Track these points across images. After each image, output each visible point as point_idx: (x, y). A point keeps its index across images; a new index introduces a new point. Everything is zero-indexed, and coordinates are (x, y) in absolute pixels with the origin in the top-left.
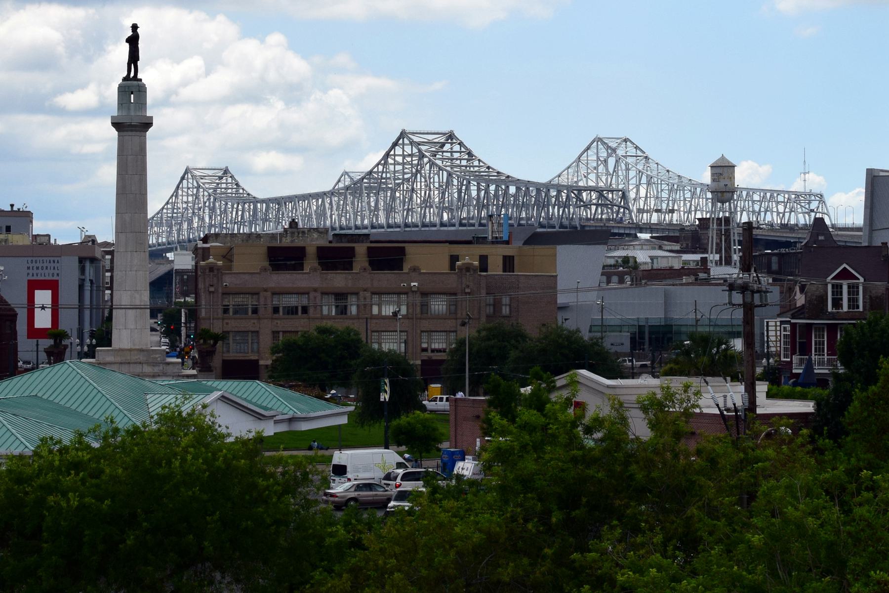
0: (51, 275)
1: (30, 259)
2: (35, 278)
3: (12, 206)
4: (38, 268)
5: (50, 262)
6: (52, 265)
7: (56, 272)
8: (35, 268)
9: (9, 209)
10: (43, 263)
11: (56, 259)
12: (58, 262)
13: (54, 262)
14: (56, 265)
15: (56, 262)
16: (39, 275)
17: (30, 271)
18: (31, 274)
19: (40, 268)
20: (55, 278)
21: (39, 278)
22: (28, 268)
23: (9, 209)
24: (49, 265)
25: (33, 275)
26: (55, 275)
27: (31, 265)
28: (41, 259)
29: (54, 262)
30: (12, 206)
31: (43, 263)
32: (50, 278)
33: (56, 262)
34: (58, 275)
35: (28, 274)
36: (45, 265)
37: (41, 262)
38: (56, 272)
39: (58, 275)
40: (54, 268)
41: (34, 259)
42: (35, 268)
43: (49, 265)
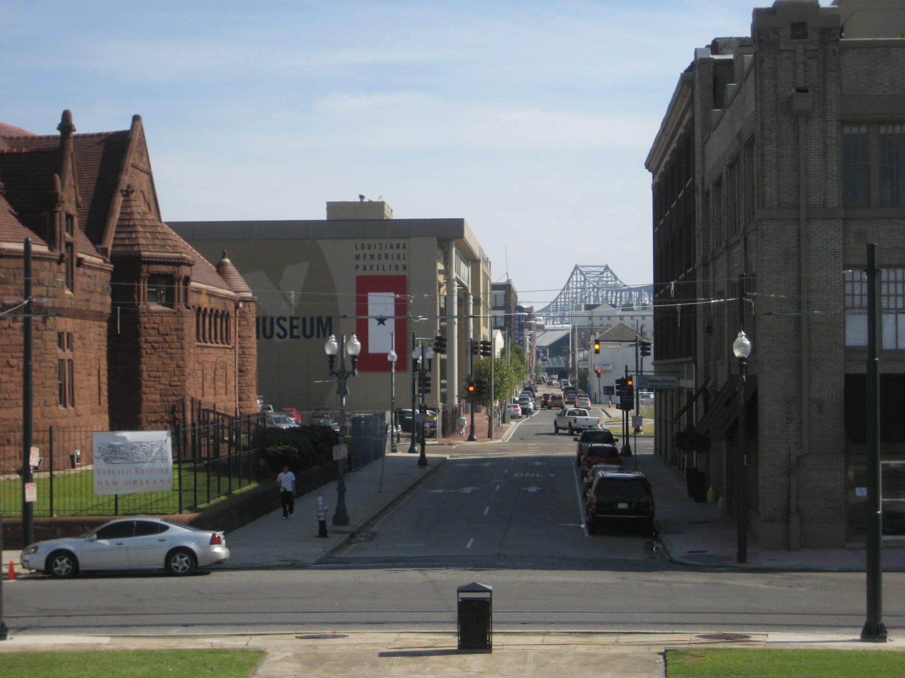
0: (393, 268)
1: (359, 242)
2: (368, 273)
3: (362, 197)
4: (372, 257)
5: (392, 247)
6: (396, 252)
7: (401, 263)
8: (368, 257)
9: (359, 200)
10: (381, 248)
11: (401, 242)
12: (404, 247)
13: (398, 246)
14: (401, 251)
15: (401, 246)
16: (375, 268)
17: (361, 263)
18: (361, 267)
19: (376, 257)
20: (401, 272)
21: (374, 273)
22: (358, 257)
23: (359, 200)
24: (390, 252)
25: (365, 269)
26: (401, 268)
27: (361, 252)
28: (377, 242)
29: (398, 246)
30: (362, 197)
31: (381, 248)
32: (394, 273)
33: (401, 246)
34: (404, 267)
35: (357, 267)
36: (383, 252)
37: (378, 247)
38: (401, 263)
39: (404, 267)
40: (398, 258)
41: (366, 242)
42: (368, 257)
43: (390, 252)
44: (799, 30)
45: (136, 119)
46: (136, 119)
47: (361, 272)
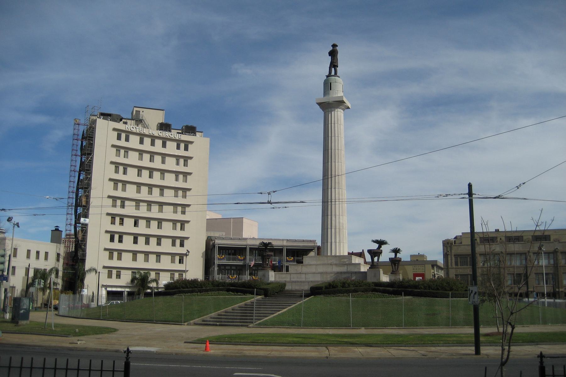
1: (414, 266)
3: (419, 253)
4: (417, 269)
8: (416, 269)
17: (414, 270)
18: (414, 271)
20: (423, 272)
21: (417, 273)
22: (413, 269)
27: (414, 268)
30: (419, 253)
32: (421, 273)
35: (413, 271)
40: (422, 269)
41: (415, 266)
42: (416, 269)
44: (448, 243)
45: (363, 250)
46: (363, 250)
47: (414, 273)
